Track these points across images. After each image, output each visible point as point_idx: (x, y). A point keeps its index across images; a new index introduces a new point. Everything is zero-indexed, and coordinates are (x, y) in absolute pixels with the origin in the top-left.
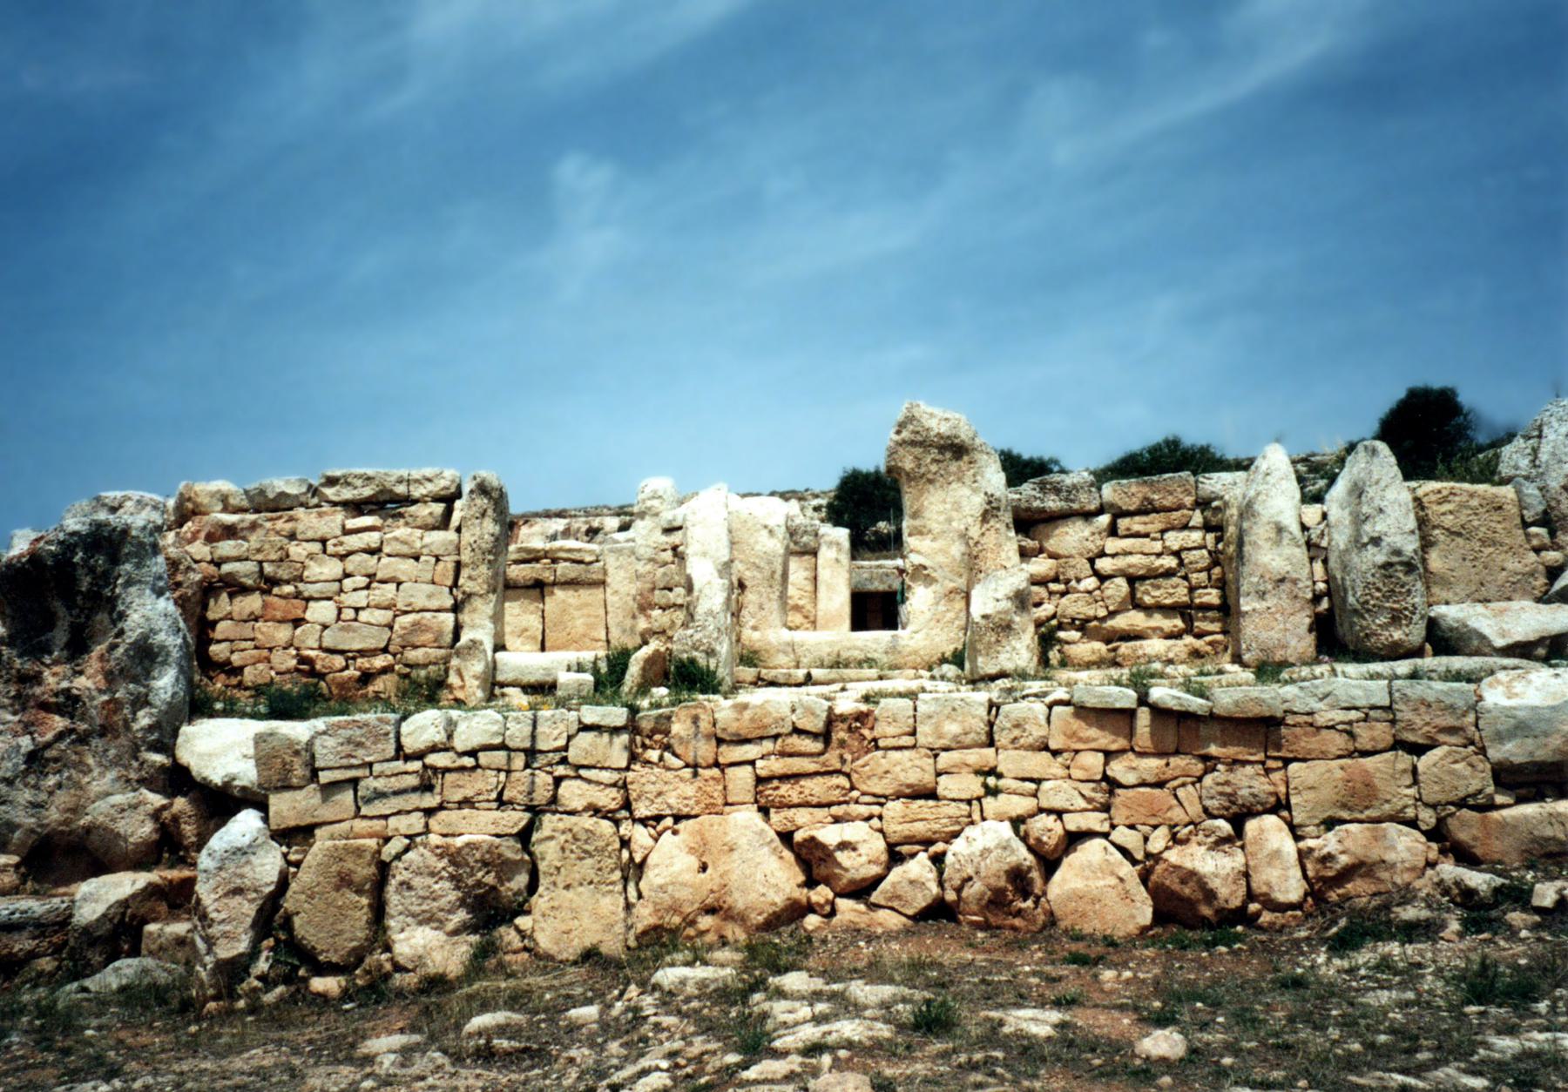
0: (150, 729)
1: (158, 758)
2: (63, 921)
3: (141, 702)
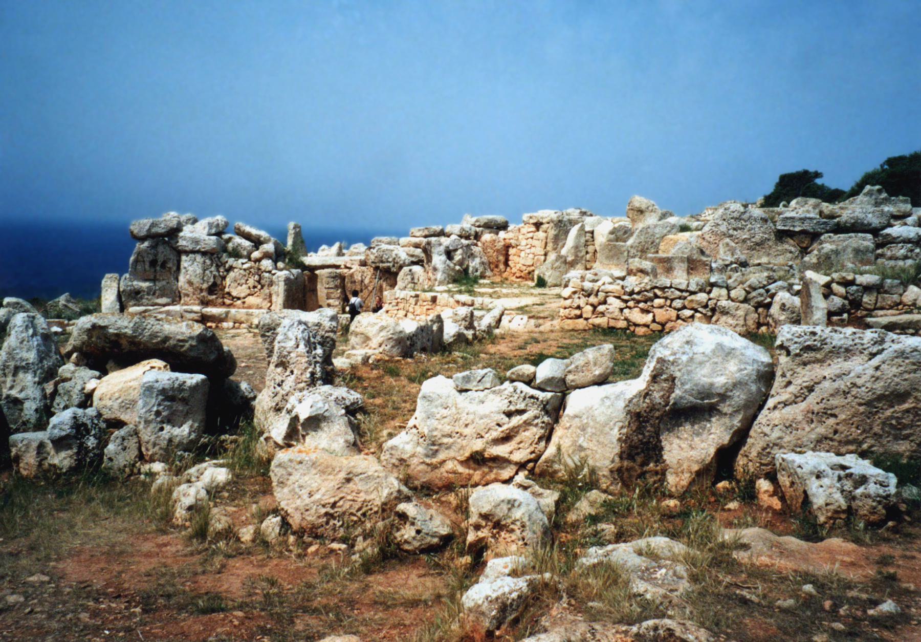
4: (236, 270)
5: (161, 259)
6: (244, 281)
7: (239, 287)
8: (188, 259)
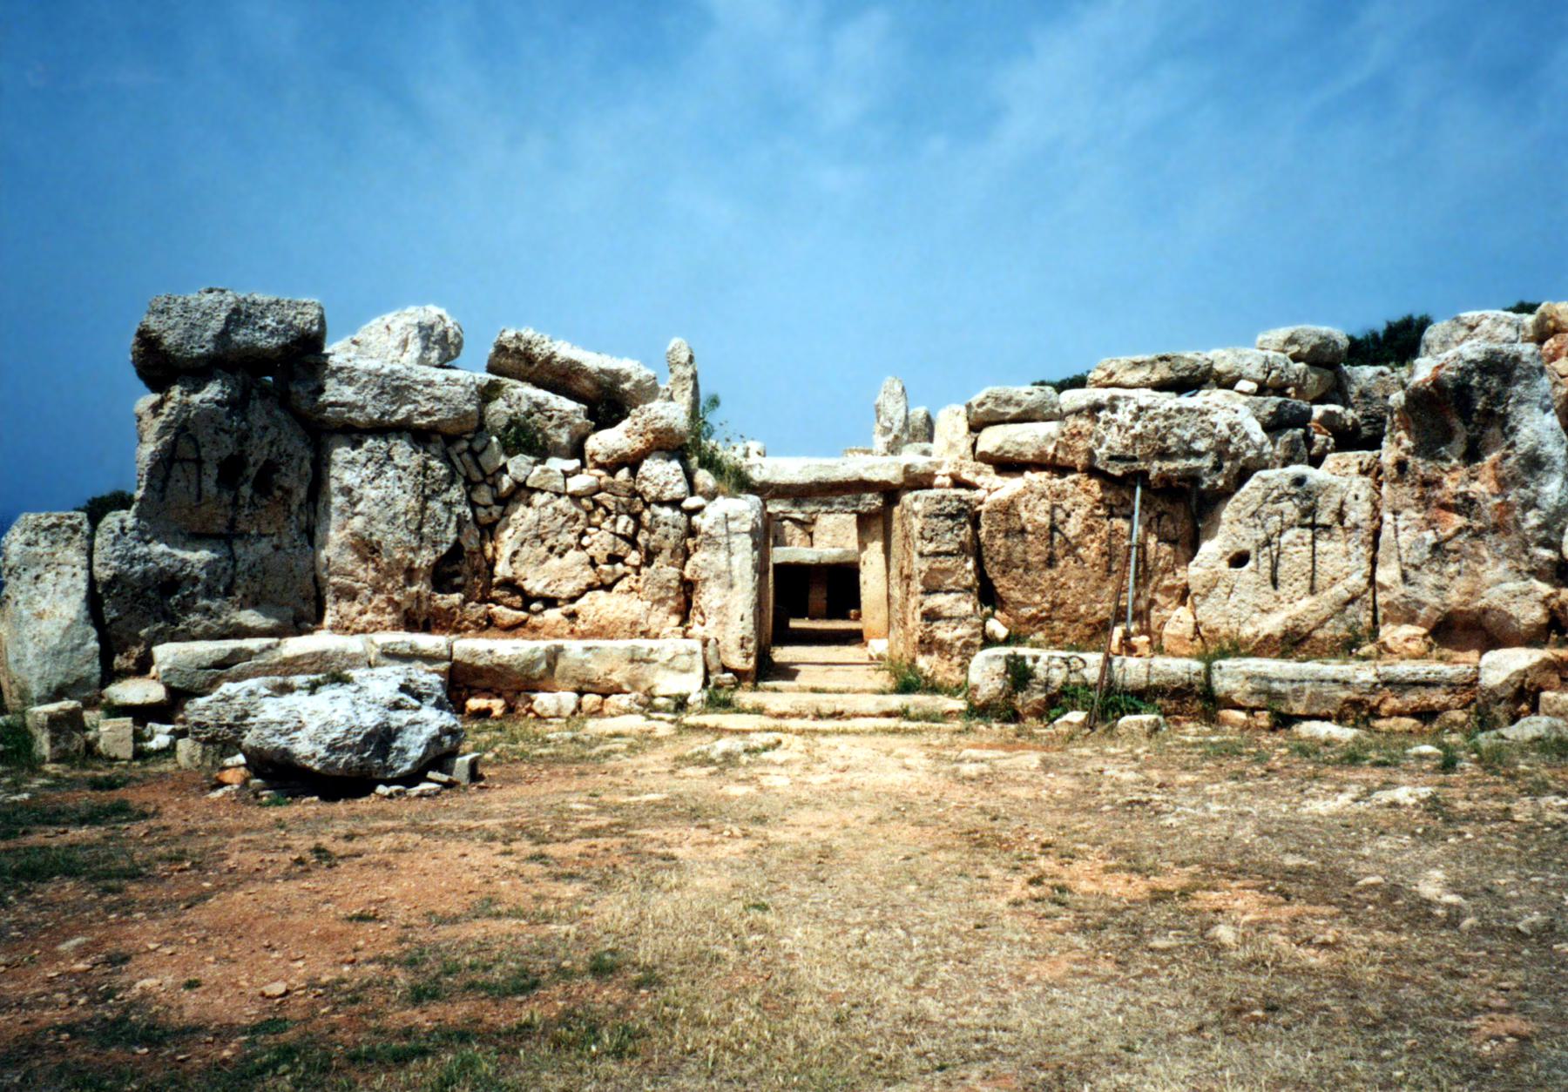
0: (1539, 528)
1: (1547, 554)
2: (1472, 683)
3: (1530, 504)
4: (538, 499)
5: (258, 454)
6: (571, 539)
7: (554, 561)
8: (360, 455)
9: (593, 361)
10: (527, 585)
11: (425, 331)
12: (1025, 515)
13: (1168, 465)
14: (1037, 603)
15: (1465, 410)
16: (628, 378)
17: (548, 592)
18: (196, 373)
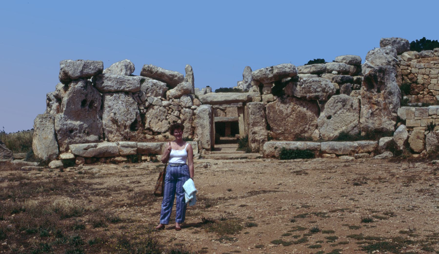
0: (393, 108)
1: (394, 114)
3: (390, 103)
4: (156, 107)
5: (89, 99)
6: (164, 117)
9: (168, 72)
10: (154, 129)
11: (126, 66)
12: (277, 108)
13: (311, 95)
14: (281, 130)
15: (376, 81)
16: (176, 76)
17: (159, 131)
18: (76, 80)
